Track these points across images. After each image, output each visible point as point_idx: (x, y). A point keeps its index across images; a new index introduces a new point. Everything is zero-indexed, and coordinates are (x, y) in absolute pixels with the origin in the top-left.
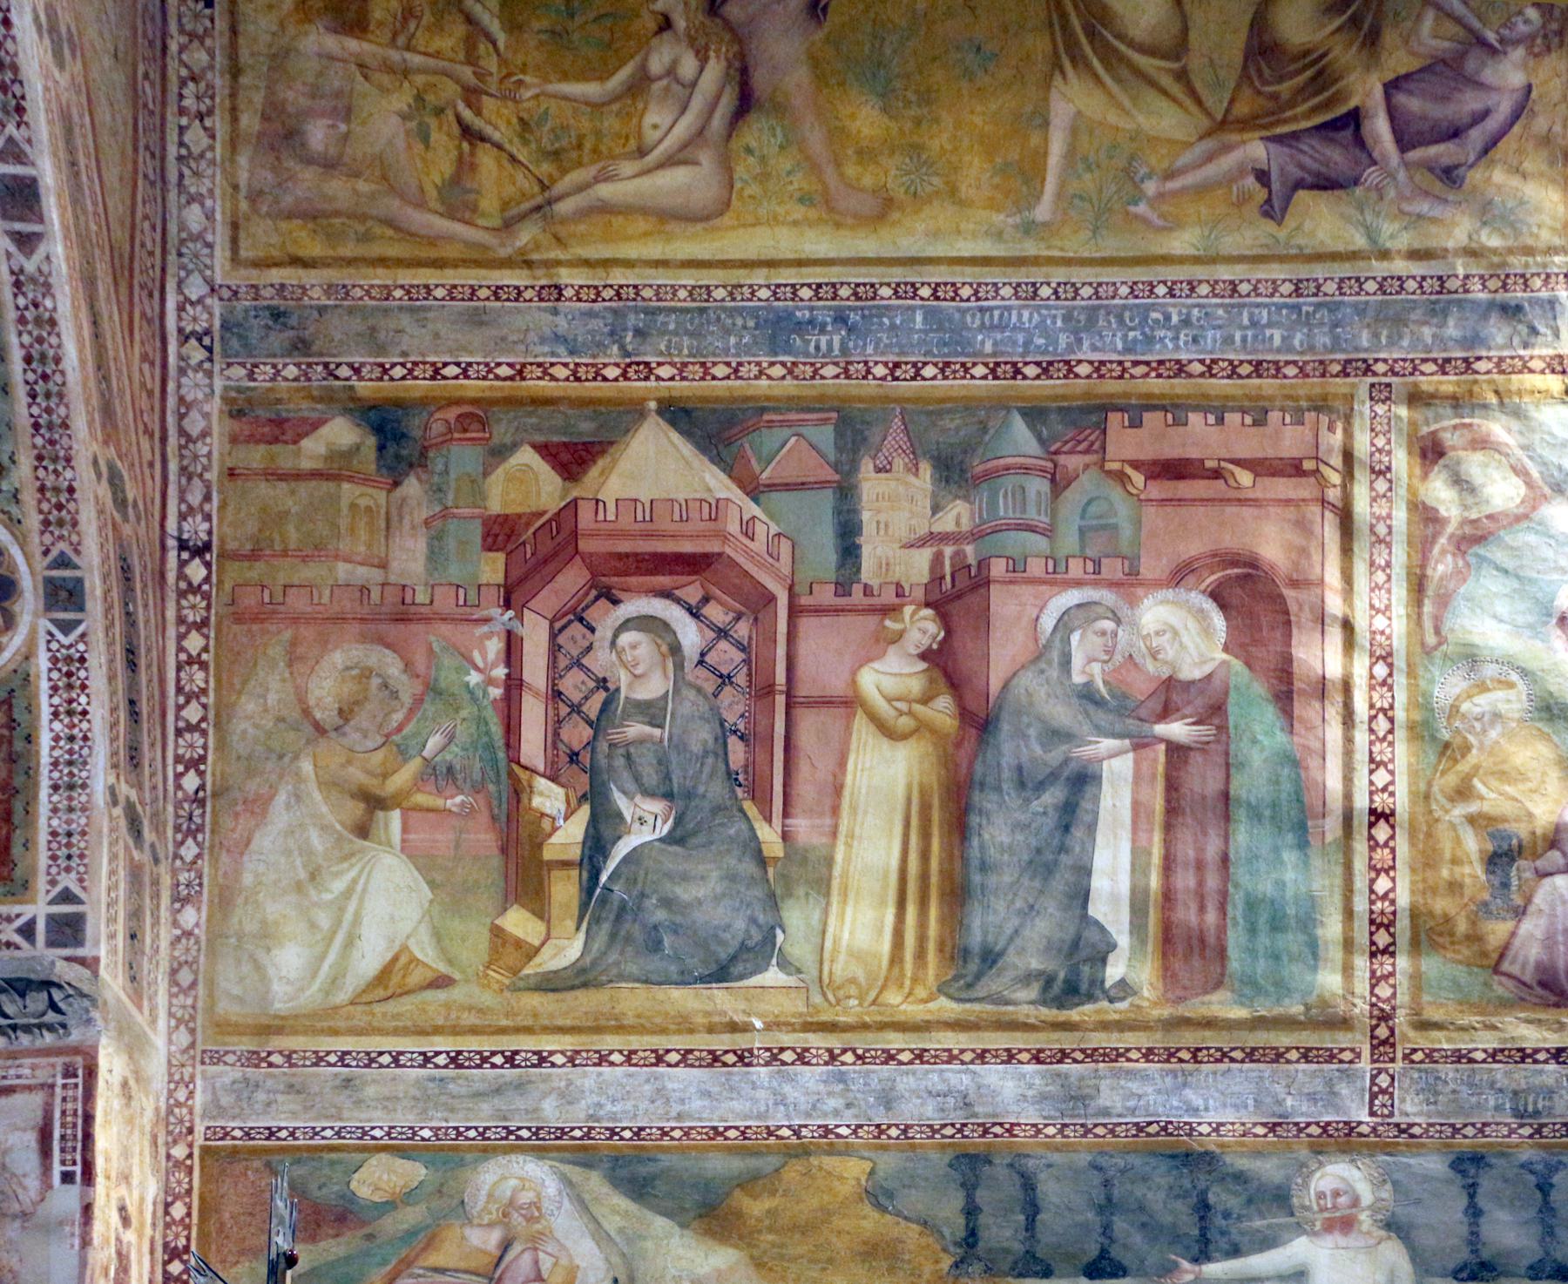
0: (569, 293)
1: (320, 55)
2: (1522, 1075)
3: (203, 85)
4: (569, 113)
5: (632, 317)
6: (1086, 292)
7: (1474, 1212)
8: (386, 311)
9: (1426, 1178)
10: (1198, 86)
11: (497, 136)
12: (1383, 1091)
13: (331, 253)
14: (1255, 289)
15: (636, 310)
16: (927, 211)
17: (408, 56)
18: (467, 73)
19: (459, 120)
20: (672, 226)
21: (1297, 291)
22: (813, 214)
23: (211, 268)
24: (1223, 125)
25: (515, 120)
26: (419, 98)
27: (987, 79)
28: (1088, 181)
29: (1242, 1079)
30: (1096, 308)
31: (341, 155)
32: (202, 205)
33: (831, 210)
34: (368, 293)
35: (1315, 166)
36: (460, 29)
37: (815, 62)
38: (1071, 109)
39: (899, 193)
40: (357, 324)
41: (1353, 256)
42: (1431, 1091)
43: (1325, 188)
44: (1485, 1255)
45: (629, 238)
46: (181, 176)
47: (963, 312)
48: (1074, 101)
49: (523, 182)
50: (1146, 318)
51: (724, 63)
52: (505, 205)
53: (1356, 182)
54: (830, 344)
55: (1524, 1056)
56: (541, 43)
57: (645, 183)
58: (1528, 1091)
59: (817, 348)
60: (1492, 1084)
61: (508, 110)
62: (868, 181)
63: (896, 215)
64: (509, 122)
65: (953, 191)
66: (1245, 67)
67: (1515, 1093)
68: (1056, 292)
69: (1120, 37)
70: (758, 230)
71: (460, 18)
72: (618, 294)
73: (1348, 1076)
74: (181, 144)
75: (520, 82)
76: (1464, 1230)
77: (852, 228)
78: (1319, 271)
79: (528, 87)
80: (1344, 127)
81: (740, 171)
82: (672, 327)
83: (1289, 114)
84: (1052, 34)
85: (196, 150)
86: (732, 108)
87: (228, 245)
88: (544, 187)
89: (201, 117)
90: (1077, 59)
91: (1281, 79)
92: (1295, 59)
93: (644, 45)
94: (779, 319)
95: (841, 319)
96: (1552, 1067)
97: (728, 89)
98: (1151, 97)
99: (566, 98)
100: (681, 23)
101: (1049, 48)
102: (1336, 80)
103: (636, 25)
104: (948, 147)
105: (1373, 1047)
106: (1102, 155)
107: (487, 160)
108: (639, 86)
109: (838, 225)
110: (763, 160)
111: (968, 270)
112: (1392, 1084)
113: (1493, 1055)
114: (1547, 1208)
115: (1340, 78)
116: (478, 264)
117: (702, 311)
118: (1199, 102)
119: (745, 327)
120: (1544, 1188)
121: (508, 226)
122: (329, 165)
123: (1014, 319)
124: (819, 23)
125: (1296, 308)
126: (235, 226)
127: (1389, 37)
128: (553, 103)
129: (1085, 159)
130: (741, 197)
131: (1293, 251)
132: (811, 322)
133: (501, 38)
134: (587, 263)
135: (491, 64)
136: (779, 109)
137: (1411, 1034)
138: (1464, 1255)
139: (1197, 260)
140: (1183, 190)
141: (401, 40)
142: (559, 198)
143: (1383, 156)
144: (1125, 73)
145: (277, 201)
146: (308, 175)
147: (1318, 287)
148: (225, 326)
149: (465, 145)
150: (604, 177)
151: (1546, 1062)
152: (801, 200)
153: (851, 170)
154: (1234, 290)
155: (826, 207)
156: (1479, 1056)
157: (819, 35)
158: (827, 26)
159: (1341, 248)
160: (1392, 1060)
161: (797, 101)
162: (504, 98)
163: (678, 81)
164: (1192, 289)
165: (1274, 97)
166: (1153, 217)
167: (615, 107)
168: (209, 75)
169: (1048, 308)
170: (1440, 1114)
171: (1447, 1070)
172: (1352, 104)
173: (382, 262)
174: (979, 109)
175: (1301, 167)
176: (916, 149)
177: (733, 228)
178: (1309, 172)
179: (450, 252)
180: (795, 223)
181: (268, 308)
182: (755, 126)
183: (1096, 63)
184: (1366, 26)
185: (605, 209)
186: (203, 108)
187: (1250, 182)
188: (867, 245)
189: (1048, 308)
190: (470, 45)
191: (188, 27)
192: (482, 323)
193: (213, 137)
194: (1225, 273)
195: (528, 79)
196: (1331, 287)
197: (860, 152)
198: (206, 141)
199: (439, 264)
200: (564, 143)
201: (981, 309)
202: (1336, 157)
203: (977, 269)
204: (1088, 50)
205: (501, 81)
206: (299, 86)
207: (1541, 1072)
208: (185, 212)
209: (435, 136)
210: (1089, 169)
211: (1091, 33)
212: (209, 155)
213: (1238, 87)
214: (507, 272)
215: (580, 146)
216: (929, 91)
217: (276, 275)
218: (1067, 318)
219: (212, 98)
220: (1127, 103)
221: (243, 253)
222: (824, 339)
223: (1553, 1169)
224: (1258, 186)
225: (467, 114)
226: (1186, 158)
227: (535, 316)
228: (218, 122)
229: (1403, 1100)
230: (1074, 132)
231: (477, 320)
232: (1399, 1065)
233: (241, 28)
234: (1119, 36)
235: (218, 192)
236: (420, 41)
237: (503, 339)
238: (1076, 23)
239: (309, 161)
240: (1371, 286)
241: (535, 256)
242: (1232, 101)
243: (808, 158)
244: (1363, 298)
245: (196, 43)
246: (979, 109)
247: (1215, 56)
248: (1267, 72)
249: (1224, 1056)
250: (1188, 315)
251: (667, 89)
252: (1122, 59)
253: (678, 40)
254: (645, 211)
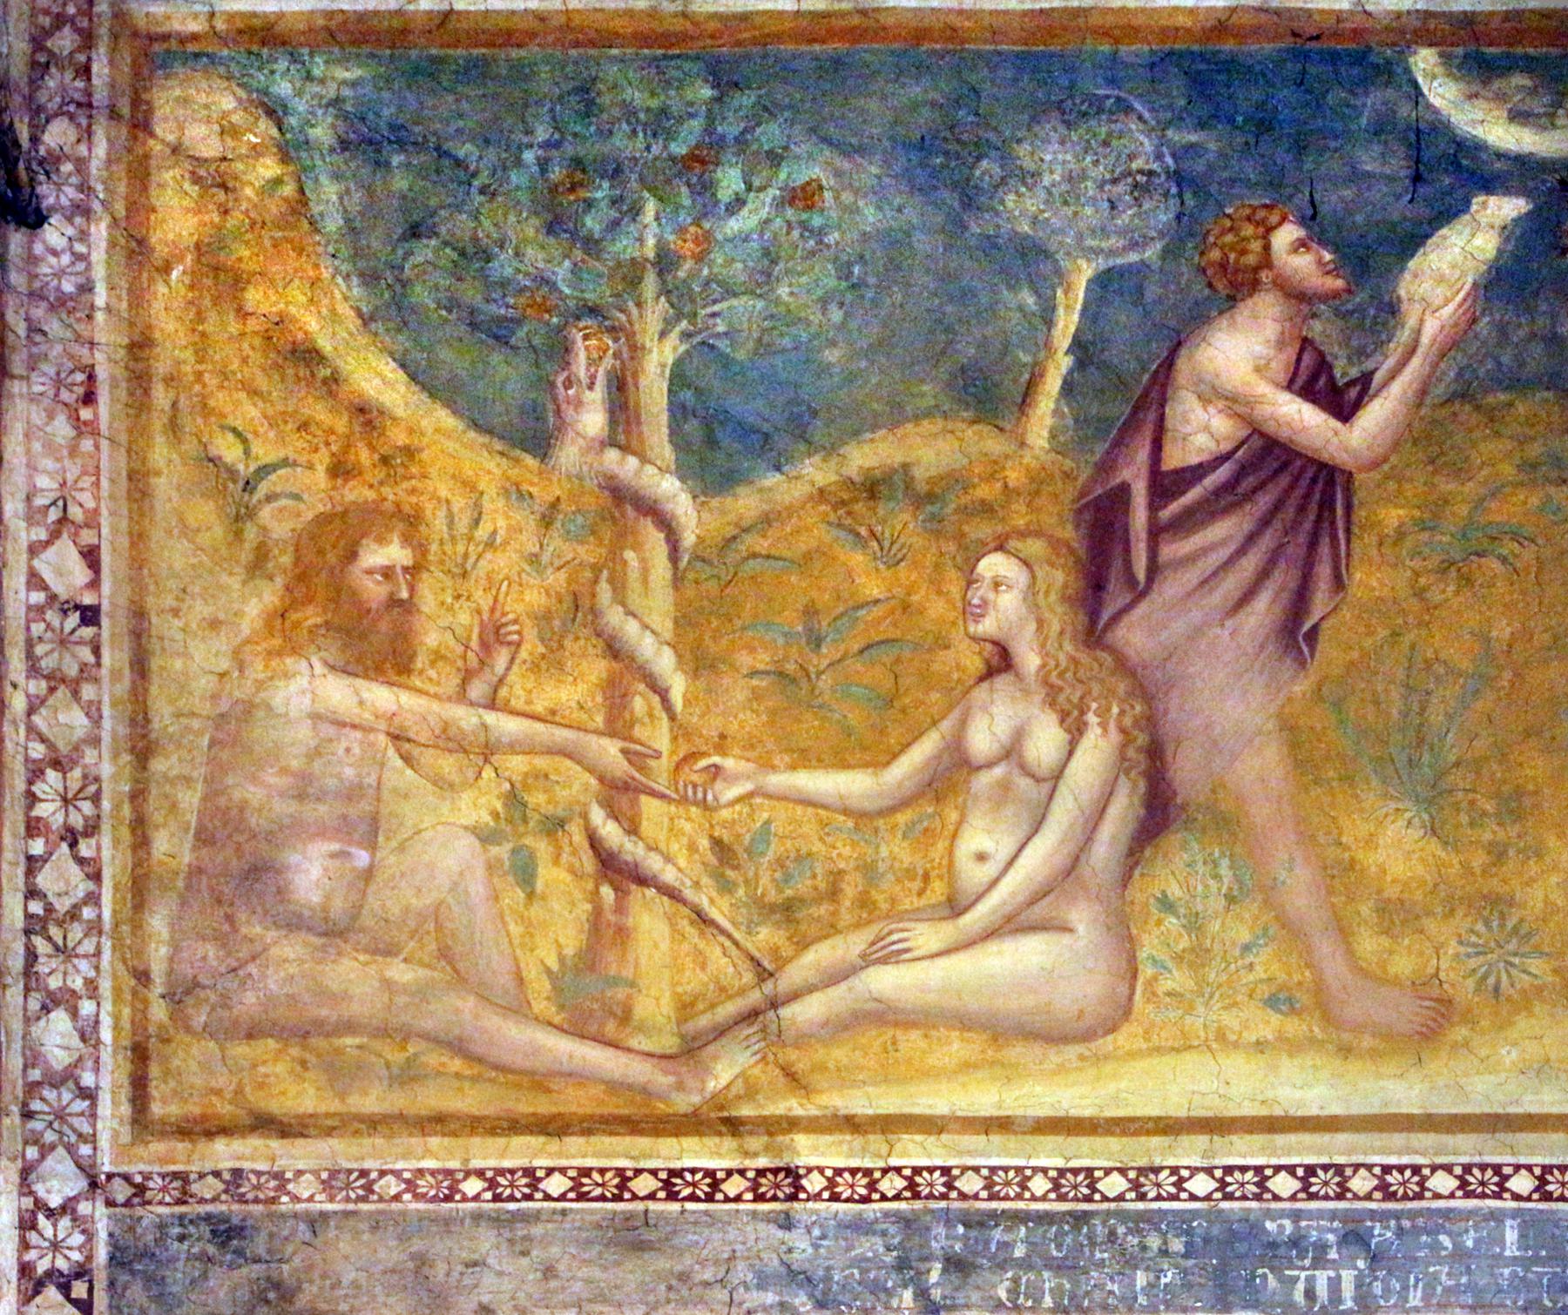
0: (814, 1183)
1: (316, 717)
3: (77, 773)
5: (941, 1230)
8: (447, 1222)
11: (669, 876)
13: (335, 1106)
15: (948, 1219)
16: (1523, 1024)
17: (491, 718)
18: (610, 751)
19: (594, 842)
20: (1017, 1052)
22: (1295, 1027)
23: (92, 1139)
25: (704, 843)
26: (513, 798)
31: (356, 911)
32: (74, 1013)
33: (1328, 1018)
34: (411, 1185)
36: (597, 668)
37: (1290, 730)
39: (1465, 991)
40: (390, 1253)
45: (929, 1074)
46: (31, 956)
49: (722, 963)
52: (686, 1007)
54: (1335, 1285)
56: (756, 695)
57: (962, 966)
59: (1310, 1294)
61: (691, 823)
62: (1403, 965)
63: (1460, 1033)
64: (692, 848)
71: (595, 647)
72: (912, 1186)
74: (32, 893)
75: (716, 771)
77: (1374, 1055)
79: (734, 779)
81: (1149, 947)
82: (1019, 1252)
85: (62, 906)
87: (125, 1094)
89: (72, 837)
93: (958, 697)
95: (1354, 1236)
100: (1030, 660)
107: (649, 921)
108: (950, 777)
109: (1346, 1051)
116: (632, 1125)
117: (1081, 1218)
119: (1164, 1252)
121: (691, 1050)
122: (333, 932)
126: (140, 1054)
132: (1296, 1242)
134: (852, 1124)
135: (659, 737)
141: (477, 690)
142: (794, 996)
145: (225, 1001)
146: (290, 951)
148: (119, 1258)
149: (607, 892)
150: (883, 954)
152: (1272, 1002)
153: (1368, 944)
161: (1260, 812)
162: (684, 800)
167: (902, 818)
168: (90, 756)
173: (438, 1123)
176: (1498, 904)
179: (575, 1101)
180: (1260, 1046)
181: (208, 1218)
182: (1180, 859)
185: (885, 1017)
186: (77, 821)
190: (615, 698)
191: (47, 664)
192: (641, 1247)
193: (96, 877)
195: (729, 763)
198: (82, 887)
199: (553, 1127)
200: (802, 886)
205: (678, 767)
206: (271, 777)
208: (37, 1030)
209: (548, 874)
212: (88, 913)
214: (690, 1142)
215: (834, 894)
217: (224, 1153)
219: (96, 799)
221: (156, 1109)
222: (1322, 1278)
225: (611, 832)
227: (747, 1229)
228: (108, 848)
231: (633, 1237)
233: (155, 663)
235: (105, 986)
236: (518, 688)
237: (684, 1277)
239: (294, 923)
241: (746, 1111)
243: (1284, 922)
245: (63, 692)
251: (1005, 786)
253: (1026, 692)
254: (964, 1022)
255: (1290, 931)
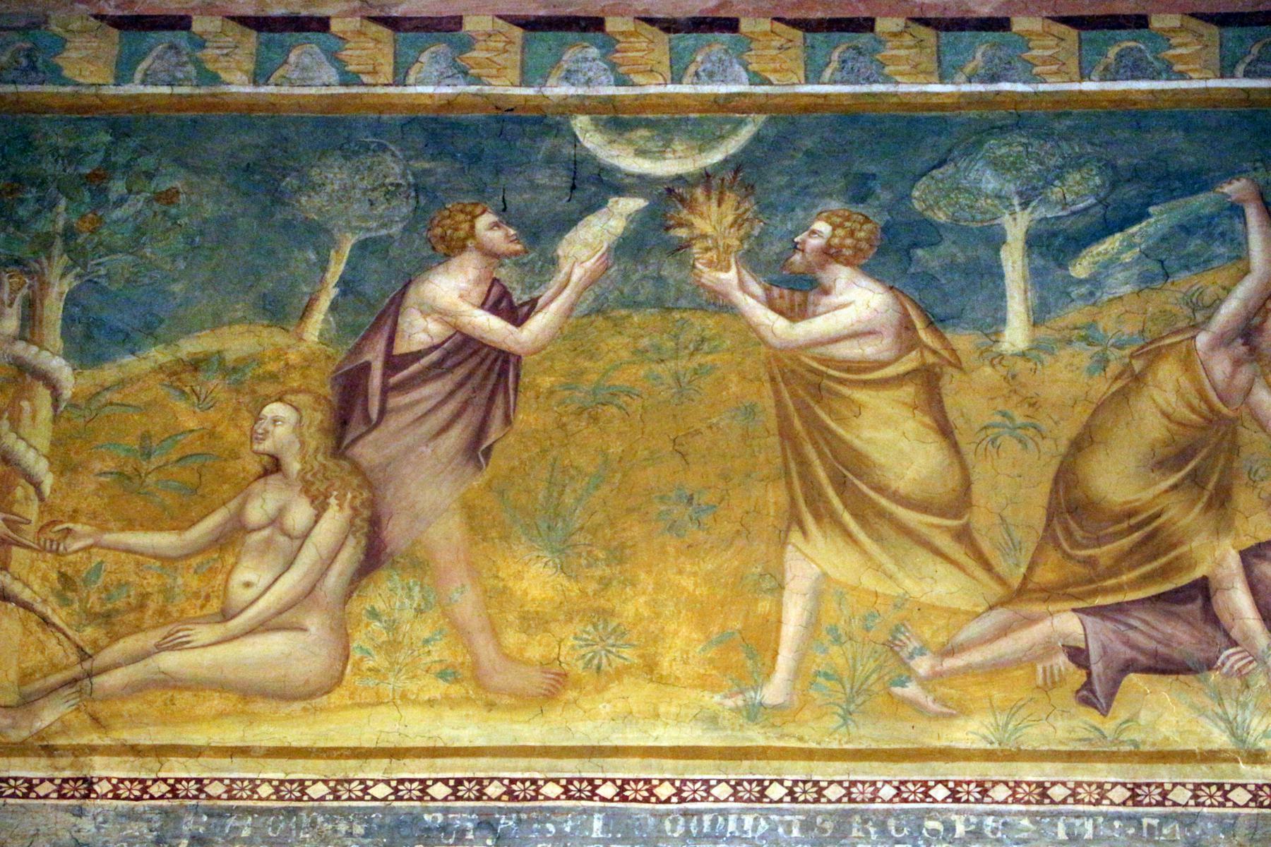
4: (130, 567)
6: (834, 792)
10: (985, 546)
11: (26, 595)
14: (1074, 794)
15: (196, 811)
16: (615, 689)
20: (260, 706)
21: (1134, 799)
22: (456, 690)
24: (1021, 593)
25: (54, 575)
27: (701, 535)
28: (838, 657)
30: (848, 814)
35: (1152, 645)
37: (470, 512)
38: (813, 571)
41: (1211, 757)
43: (1164, 672)
45: (195, 720)
47: (661, 816)
48: (816, 562)
50: (920, 827)
51: (348, 512)
52: (25, 677)
53: (1210, 665)
56: (102, 486)
61: (48, 565)
62: (535, 652)
63: (571, 694)
64: (45, 578)
65: (650, 668)
66: (1048, 525)
68: (791, 792)
69: (880, 490)
70: (382, 709)
72: (173, 790)
75: (69, 531)
77: (511, 708)
78: (1164, 774)
80: (1192, 599)
81: (359, 640)
82: (246, 833)
83: (1111, 582)
84: (789, 485)
86: (350, 570)
88: (84, 656)
90: (823, 514)
91: (1099, 542)
92: (1118, 519)
93: (243, 489)
94: (400, 824)
97: (351, 542)
98: (922, 557)
99: (129, 551)
100: (294, 466)
101: (784, 499)
102: (1174, 546)
103: (232, 467)
104: (646, 613)
106: (856, 623)
108: (232, 537)
109: (490, 706)
110: (392, 626)
111: (669, 763)
115: (1180, 543)
118: (988, 566)
119: (350, 834)
123: (732, 826)
124: (479, 468)
125: (1135, 820)
127: (1243, 498)
128: (111, 556)
129: (833, 630)
130: (357, 665)
131: (1128, 748)
132: (444, 828)
133: (48, 482)
136: (418, 564)
139: (988, 756)
140: (967, 670)
142: (105, 670)
143: (1246, 637)
144: (886, 530)
147: (1164, 795)
152: (442, 675)
153: (512, 638)
154: (1044, 795)
155: (474, 683)
157: (478, 481)
158: (487, 473)
159: (1193, 746)
161: (444, 557)
162: (43, 549)
163: (285, 533)
164: (984, 792)
165: (1090, 562)
166: (928, 701)
169: (780, 812)
172: (1198, 573)
174: (688, 568)
175: (1128, 643)
177: (345, 708)
178: (1142, 651)
180: (431, 703)
183: (847, 518)
184: (1211, 486)
185: (169, 683)
187: (1062, 660)
188: (530, 731)
189: (780, 812)
194: (1030, 772)
195: (78, 527)
196: (1182, 795)
197: (524, 617)
200: (120, 604)
201: (685, 813)
202: (1180, 636)
203: (682, 762)
204: (836, 502)
210: (837, 640)
211: (841, 485)
213: (1039, 549)
214: (16, 761)
215: (142, 607)
216: (622, 546)
218: (807, 826)
220: (890, 566)
224: (1072, 667)
226: (974, 630)
230: (818, 596)
234: (880, 490)
238: (822, 475)
240: (1240, 796)
241: (61, 741)
242: (1031, 568)
243: (454, 624)
244: (1229, 810)
246: (688, 568)
247: (1007, 513)
248: (1079, 534)
250: (980, 825)
251: (269, 542)
252: (882, 514)
253: (289, 485)
254: (221, 686)
255: (459, 632)
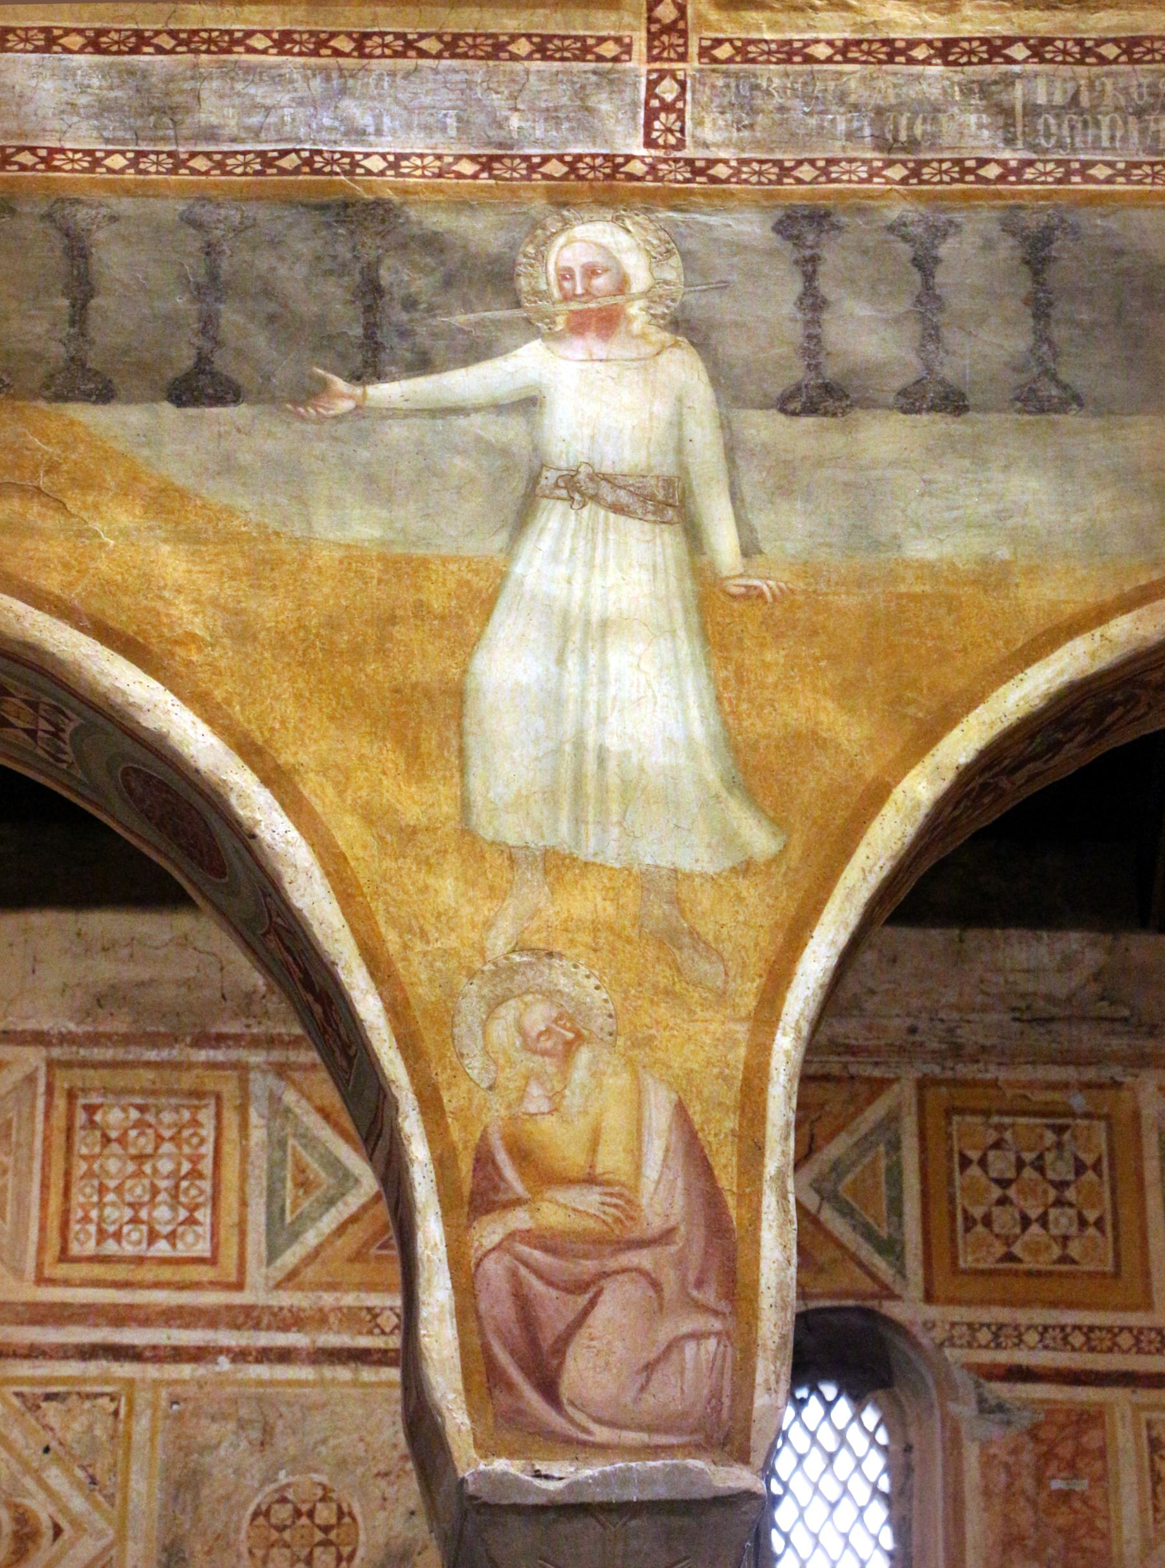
2: (888, 83)
7: (813, 303)
9: (739, 248)
12: (667, 108)
29: (438, 84)
42: (744, 108)
44: (831, 371)
55: (894, 51)
58: (898, 108)
60: (842, 98)
67: (879, 111)
73: (612, 82)
76: (795, 332)
96: (936, 69)
105: (652, 37)
112: (681, 96)
113: (845, 50)
114: (929, 298)
120: (925, 264)
137: (713, 15)
138: (797, 373)
151: (927, 62)
156: (822, 51)
160: (683, 57)
170: (757, 144)
171: (771, 74)
207: (918, 78)
223: (940, 232)
229: (699, 123)
232: (694, 64)
249: (408, 47)
